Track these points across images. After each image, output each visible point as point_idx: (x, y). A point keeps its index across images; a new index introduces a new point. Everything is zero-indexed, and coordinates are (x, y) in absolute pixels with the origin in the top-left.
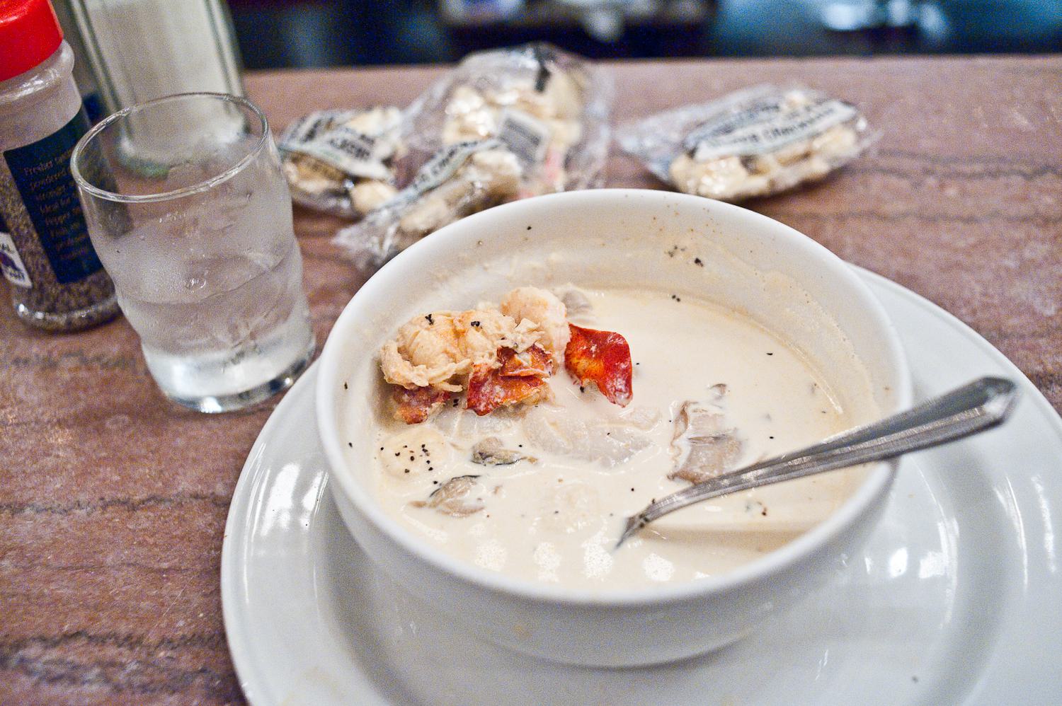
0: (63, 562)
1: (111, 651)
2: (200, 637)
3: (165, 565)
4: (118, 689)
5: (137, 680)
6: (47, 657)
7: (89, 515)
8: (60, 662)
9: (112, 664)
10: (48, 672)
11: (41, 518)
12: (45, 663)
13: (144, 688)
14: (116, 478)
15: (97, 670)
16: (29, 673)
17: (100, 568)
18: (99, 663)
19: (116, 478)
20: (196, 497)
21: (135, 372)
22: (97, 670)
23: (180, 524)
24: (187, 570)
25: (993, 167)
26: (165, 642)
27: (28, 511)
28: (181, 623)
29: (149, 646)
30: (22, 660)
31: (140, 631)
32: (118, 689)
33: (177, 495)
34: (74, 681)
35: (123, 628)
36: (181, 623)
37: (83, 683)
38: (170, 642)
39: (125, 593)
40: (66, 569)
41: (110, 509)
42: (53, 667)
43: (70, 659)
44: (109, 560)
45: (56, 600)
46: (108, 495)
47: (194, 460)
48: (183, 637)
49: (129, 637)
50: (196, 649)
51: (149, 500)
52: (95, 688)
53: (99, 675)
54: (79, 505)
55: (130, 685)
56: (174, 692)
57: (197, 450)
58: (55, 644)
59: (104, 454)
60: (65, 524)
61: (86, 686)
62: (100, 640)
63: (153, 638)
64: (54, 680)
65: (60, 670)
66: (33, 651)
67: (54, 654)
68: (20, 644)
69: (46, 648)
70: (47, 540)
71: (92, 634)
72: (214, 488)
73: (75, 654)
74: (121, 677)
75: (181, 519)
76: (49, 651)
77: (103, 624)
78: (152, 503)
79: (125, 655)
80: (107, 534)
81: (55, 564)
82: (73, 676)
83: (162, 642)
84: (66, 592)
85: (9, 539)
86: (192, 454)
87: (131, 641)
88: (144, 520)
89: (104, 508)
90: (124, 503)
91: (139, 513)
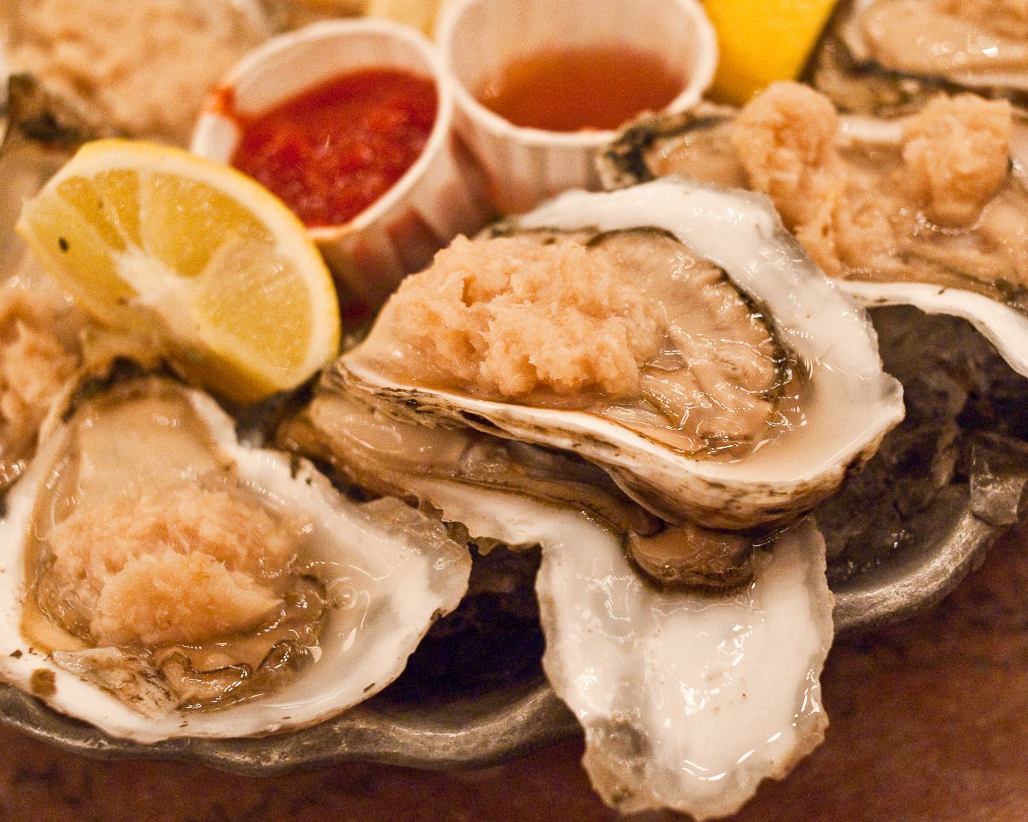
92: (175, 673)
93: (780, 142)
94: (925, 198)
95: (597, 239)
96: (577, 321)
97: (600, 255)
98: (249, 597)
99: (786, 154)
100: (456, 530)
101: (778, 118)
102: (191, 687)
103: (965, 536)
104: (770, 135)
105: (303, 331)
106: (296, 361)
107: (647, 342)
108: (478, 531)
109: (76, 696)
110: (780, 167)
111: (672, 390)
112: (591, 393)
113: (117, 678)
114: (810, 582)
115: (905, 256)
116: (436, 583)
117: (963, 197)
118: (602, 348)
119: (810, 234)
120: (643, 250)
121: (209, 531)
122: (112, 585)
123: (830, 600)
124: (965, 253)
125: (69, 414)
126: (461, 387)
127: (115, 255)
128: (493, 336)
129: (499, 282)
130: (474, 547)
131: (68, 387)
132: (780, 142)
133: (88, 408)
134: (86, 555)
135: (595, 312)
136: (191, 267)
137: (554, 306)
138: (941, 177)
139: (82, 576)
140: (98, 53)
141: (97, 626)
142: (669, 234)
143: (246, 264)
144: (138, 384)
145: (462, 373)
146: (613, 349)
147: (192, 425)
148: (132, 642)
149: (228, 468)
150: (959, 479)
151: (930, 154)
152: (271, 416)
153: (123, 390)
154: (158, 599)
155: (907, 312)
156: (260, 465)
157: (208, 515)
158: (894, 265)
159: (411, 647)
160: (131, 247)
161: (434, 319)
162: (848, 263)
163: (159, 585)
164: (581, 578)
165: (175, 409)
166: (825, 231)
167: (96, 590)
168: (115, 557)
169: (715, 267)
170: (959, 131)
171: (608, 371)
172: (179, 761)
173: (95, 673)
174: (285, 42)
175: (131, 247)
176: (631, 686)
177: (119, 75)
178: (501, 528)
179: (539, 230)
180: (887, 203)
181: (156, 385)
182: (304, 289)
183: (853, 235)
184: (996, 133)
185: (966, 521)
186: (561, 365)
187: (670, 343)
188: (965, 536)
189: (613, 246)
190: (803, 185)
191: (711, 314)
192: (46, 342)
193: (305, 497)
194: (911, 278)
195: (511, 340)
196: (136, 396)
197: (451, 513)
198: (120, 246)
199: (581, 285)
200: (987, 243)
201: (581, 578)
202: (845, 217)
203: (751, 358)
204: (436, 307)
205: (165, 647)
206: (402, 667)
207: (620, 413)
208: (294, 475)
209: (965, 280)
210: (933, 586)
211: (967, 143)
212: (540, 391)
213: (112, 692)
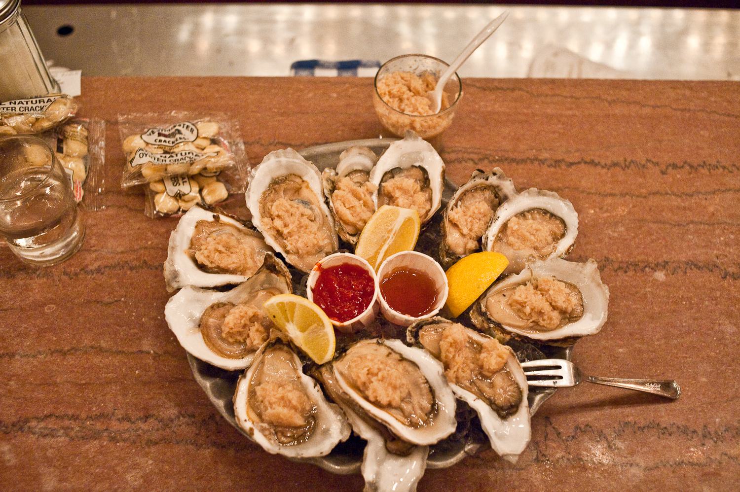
0: (38, 382)
1: (67, 423)
2: (103, 415)
3: (84, 382)
4: (72, 439)
5: (80, 434)
6: (39, 426)
7: (45, 358)
8: (45, 428)
9: (68, 428)
10: (42, 432)
11: (24, 360)
12: (39, 429)
13: (83, 438)
14: (54, 339)
15: (62, 431)
16: (34, 434)
17: (55, 384)
18: (63, 428)
19: (54, 339)
20: (92, 347)
21: (54, 280)
22: (62, 431)
23: (87, 361)
24: (93, 384)
25: (460, 156)
26: (89, 417)
27: (17, 357)
28: (94, 409)
29: (82, 420)
30: (29, 428)
31: (78, 413)
32: (72, 439)
33: (84, 347)
34: (53, 436)
35: (70, 412)
36: (94, 409)
37: (57, 437)
38: (91, 417)
39: (68, 395)
40: (40, 385)
41: (54, 355)
42: (43, 431)
43: (50, 426)
44: (58, 380)
45: (39, 400)
46: (53, 347)
47: (89, 329)
48: (96, 415)
49: (73, 416)
50: (102, 420)
51: (72, 349)
52: (62, 439)
53: (63, 433)
54: (39, 352)
55: (77, 437)
56: (96, 439)
57: (89, 323)
58: (42, 420)
59: (47, 326)
60: (35, 363)
61: (59, 438)
62: (61, 418)
63: (83, 416)
64: (45, 436)
65: (46, 432)
66: (33, 423)
67: (42, 425)
68: (27, 421)
69: (39, 422)
70: (29, 371)
71: (57, 415)
72: (99, 343)
73: (51, 424)
74: (73, 434)
75: (87, 359)
76: (40, 423)
77: (61, 410)
78: (73, 351)
79: (73, 424)
80: (56, 367)
81: (35, 383)
82: (52, 434)
83: (88, 417)
84: (42, 396)
85: (11, 371)
86: (88, 326)
87: (75, 418)
88: (70, 360)
89: (51, 354)
90: (60, 352)
91: (68, 356)
92: (279, 434)
93: (451, 346)
94: (481, 367)
95: (402, 359)
96: (390, 390)
97: (401, 367)
98: (299, 421)
99: (451, 350)
100: (350, 426)
101: (452, 341)
102: (283, 439)
103: (461, 455)
104: (449, 345)
105: (325, 352)
106: (322, 358)
107: (404, 395)
108: (355, 430)
109: (259, 438)
110: (450, 353)
111: (407, 407)
112: (387, 407)
113: (267, 433)
114: (423, 459)
115: (473, 383)
116: (341, 432)
117: (489, 372)
118: (394, 399)
119: (451, 373)
120: (411, 369)
121: (294, 402)
122: (270, 411)
123: (426, 461)
124: (484, 386)
125: (263, 353)
126: (361, 390)
127: (286, 323)
128: (371, 386)
129: (375, 371)
130: (353, 432)
131: (265, 344)
132: (451, 346)
133: (268, 350)
134: (264, 398)
135: (395, 388)
136: (303, 330)
137: (386, 385)
138: (486, 367)
139: (262, 402)
140: (286, 226)
141: (263, 417)
142: (419, 368)
143: (315, 332)
144: (282, 346)
145: (361, 389)
146: (396, 398)
147: (292, 360)
148: (271, 423)
149: (299, 378)
150: (467, 437)
151: (485, 359)
152: (311, 368)
153: (277, 346)
154: (279, 418)
155: (466, 404)
156: (307, 380)
157: (294, 396)
158: (467, 383)
159: (333, 446)
160: (290, 322)
161: (358, 377)
162: (458, 382)
163: (281, 416)
164: (375, 445)
165: (289, 357)
166: (455, 372)
167: (266, 409)
168: (271, 401)
169: (426, 379)
170: (494, 356)
171: (394, 404)
172: (279, 456)
173: (262, 430)
174: (339, 254)
175: (290, 322)
176: (378, 474)
177: (290, 234)
178: (360, 431)
179: (389, 348)
180: (472, 366)
181: (286, 348)
182: (328, 341)
183: (461, 374)
184: (503, 359)
185: (462, 452)
186: (384, 400)
187: (409, 394)
188: (461, 455)
189: (405, 364)
190: (454, 357)
191: (421, 391)
192: (261, 329)
193: (315, 393)
194: (470, 390)
195: (375, 391)
196: (280, 349)
197: (350, 421)
198: (288, 322)
199: (394, 382)
200: (492, 385)
201: (375, 445)
202: (460, 371)
203: (427, 404)
204: (360, 375)
205: (278, 428)
206: (330, 451)
207: (393, 411)
208: (315, 387)
209: (480, 395)
210: (450, 465)
211: (495, 361)
212: (377, 404)
213: (265, 436)
